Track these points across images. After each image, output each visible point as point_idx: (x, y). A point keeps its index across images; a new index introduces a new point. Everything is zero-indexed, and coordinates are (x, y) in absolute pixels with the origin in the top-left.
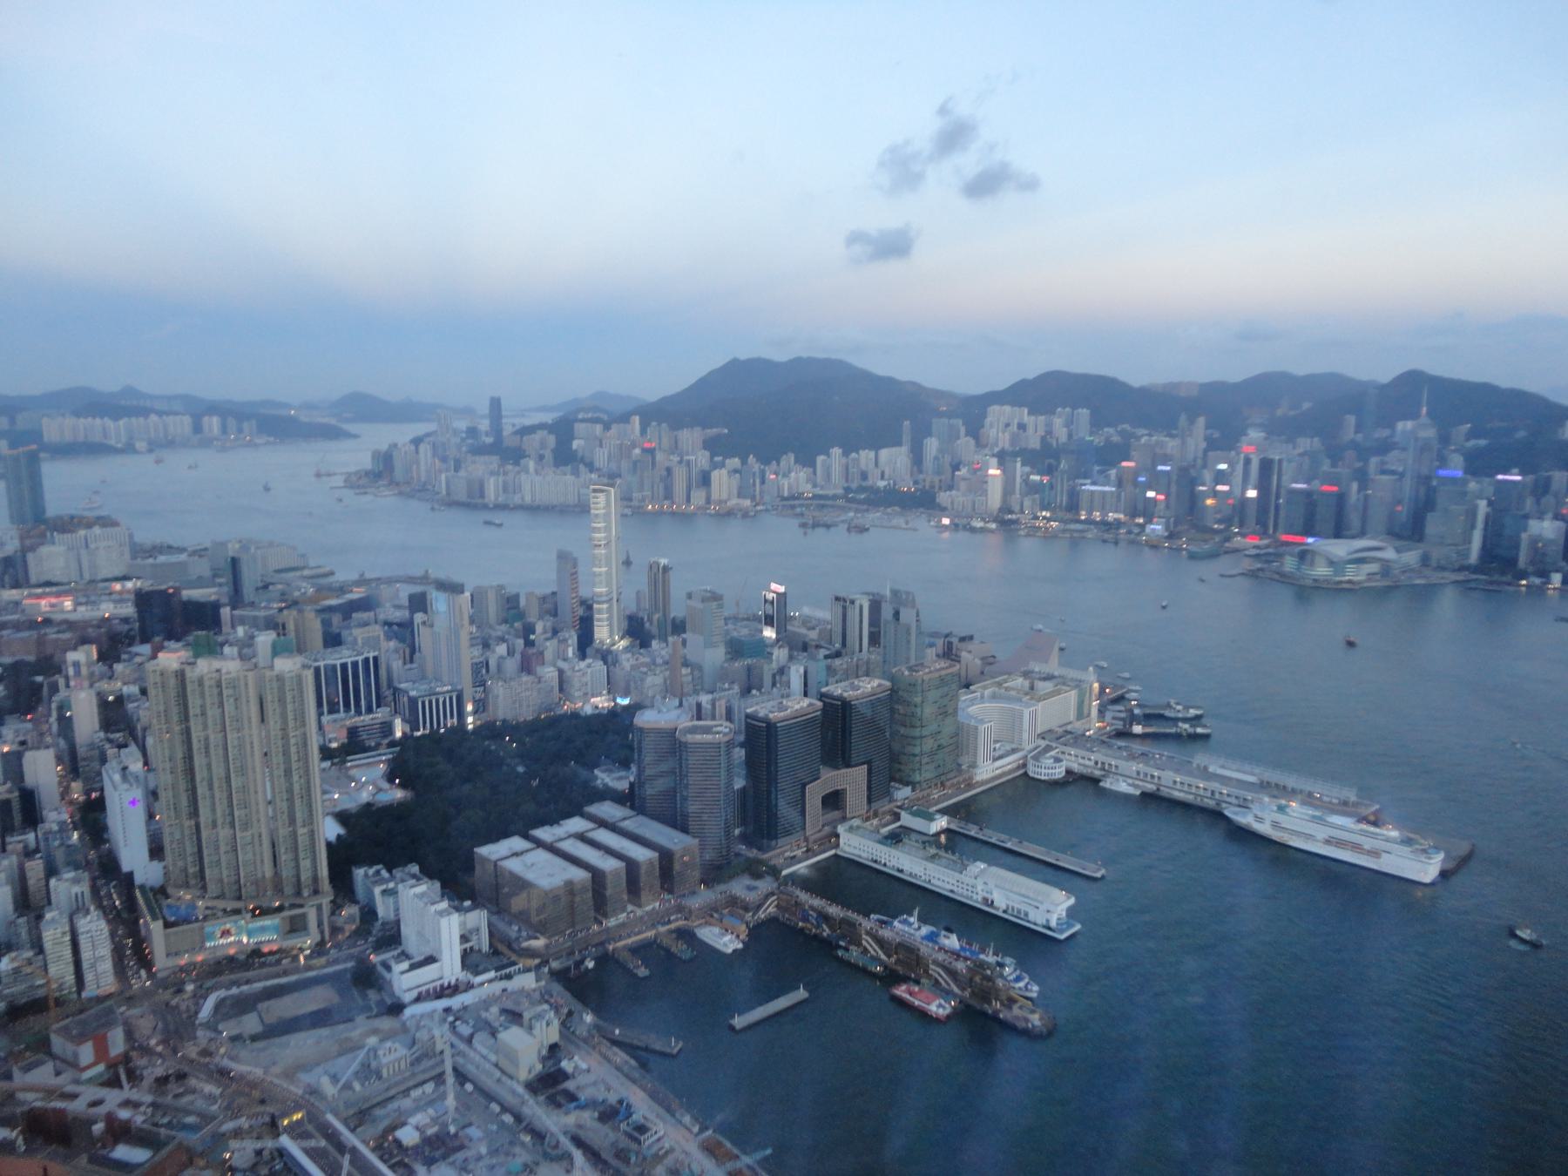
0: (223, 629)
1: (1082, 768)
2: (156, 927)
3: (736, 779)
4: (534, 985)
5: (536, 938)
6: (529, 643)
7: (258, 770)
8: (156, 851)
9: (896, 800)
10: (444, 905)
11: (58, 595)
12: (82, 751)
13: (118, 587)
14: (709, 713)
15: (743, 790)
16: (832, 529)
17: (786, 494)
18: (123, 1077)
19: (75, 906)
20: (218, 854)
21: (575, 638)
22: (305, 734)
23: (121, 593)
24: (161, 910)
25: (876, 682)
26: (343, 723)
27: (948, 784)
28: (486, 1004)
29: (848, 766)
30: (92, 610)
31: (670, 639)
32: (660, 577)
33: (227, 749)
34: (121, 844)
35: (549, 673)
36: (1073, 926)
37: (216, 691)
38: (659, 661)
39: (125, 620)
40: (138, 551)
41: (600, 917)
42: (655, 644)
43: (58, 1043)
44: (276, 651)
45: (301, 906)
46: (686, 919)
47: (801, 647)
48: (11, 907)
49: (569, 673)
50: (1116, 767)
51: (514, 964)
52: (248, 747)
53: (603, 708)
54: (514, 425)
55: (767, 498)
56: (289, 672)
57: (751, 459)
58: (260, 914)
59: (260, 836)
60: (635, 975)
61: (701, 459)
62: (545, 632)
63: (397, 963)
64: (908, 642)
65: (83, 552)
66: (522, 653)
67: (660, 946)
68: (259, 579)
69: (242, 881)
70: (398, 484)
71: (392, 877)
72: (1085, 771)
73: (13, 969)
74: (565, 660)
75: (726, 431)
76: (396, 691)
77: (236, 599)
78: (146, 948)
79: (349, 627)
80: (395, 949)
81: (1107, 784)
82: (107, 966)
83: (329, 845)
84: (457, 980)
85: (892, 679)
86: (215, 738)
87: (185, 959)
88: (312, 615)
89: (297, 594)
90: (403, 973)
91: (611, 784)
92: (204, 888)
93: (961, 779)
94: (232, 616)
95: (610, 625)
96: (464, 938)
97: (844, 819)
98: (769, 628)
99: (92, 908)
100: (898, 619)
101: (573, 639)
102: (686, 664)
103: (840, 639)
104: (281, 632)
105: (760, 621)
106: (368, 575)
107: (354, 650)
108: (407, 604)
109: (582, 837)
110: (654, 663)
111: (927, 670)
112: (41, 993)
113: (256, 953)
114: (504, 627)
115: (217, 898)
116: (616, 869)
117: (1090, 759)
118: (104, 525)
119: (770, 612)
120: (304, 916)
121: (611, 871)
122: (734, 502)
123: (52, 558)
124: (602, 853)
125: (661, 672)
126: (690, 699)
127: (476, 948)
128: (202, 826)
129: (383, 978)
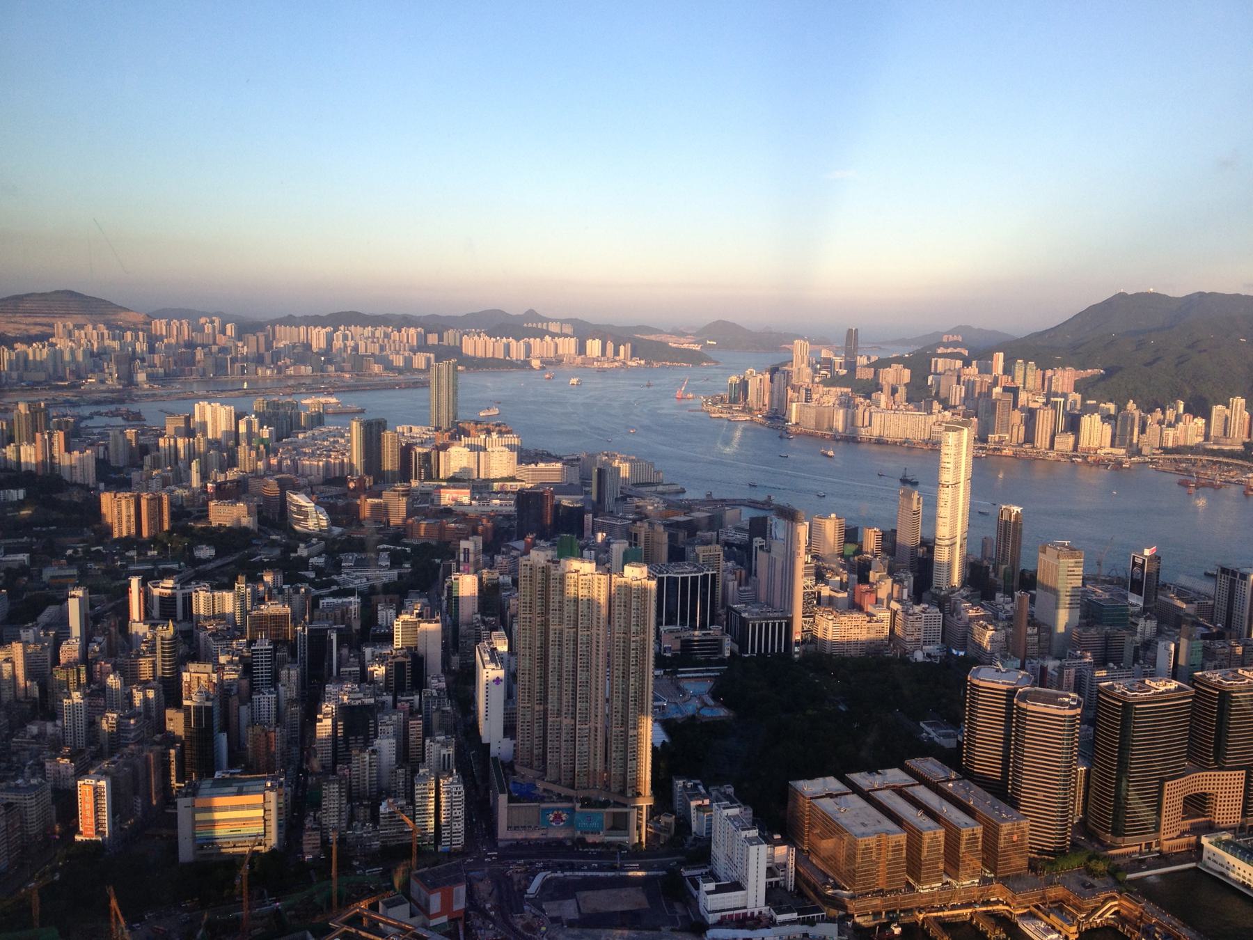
2: (503, 799)
7: (600, 668)
8: (510, 730)
10: (754, 833)
12: (462, 629)
14: (1055, 679)
17: (1170, 444)
18: (461, 933)
21: (912, 578)
22: (644, 640)
24: (508, 785)
31: (1017, 594)
39: (508, 517)
41: (911, 881)
42: (999, 597)
43: (415, 885)
44: (628, 559)
45: (625, 806)
46: (1007, 904)
51: (818, 910)
53: (935, 657)
55: (1146, 451)
57: (1131, 405)
58: (588, 806)
59: (596, 731)
67: (975, 928)
68: (619, 490)
69: (576, 770)
71: (708, 795)
73: (390, 813)
75: (1102, 371)
77: (598, 507)
79: (694, 545)
82: (460, 826)
84: (760, 913)
86: (568, 632)
87: (520, 835)
88: (662, 528)
90: (709, 893)
91: (936, 739)
92: (545, 771)
94: (593, 520)
96: (771, 871)
99: (454, 771)
101: (909, 581)
102: (1032, 622)
103: (1223, 617)
105: (1125, 587)
106: (715, 496)
107: (695, 566)
109: (900, 791)
110: (996, 618)
112: (407, 839)
113: (582, 841)
115: (554, 782)
119: (1139, 577)
120: (626, 815)
125: (1003, 628)
126: (1035, 662)
127: (782, 883)
128: (549, 712)
129: (693, 896)
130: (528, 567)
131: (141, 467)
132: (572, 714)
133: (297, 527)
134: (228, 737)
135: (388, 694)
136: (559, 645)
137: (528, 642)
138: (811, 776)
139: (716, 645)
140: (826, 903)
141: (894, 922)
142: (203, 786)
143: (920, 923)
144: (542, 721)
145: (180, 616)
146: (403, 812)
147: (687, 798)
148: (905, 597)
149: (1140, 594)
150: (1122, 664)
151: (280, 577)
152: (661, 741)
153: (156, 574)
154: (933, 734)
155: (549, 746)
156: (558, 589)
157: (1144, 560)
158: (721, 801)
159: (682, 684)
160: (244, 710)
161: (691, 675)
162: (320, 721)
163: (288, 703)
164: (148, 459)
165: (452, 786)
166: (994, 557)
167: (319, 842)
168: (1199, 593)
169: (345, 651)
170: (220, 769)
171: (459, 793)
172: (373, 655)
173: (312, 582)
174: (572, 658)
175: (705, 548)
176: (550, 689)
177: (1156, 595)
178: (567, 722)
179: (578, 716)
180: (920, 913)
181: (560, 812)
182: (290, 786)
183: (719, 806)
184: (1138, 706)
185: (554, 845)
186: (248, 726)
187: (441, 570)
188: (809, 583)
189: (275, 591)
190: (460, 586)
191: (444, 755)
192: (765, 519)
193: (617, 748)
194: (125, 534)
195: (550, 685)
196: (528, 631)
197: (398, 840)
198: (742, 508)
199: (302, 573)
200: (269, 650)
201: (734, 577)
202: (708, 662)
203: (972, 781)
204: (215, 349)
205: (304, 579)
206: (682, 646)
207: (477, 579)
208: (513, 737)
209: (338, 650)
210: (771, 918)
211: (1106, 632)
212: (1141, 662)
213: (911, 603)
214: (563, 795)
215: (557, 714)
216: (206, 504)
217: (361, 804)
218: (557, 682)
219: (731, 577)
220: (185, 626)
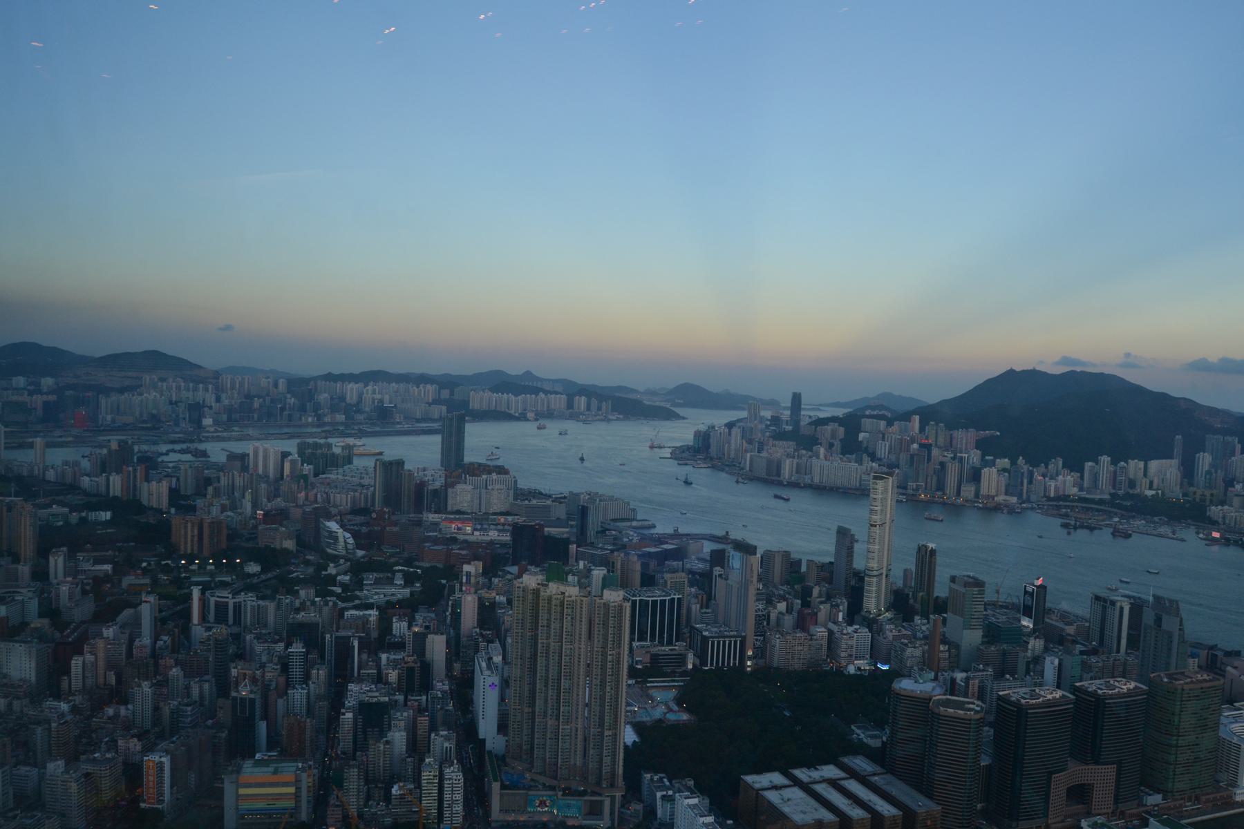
0: (570, 560)
2: (496, 786)
3: (983, 756)
6: (806, 604)
7: (581, 677)
8: (502, 728)
9: (1146, 805)
11: (464, 521)
12: (464, 639)
15: (989, 767)
16: (1096, 532)
17: (1052, 495)
19: (444, 759)
21: (846, 604)
22: (619, 654)
23: (504, 525)
25: (1132, 685)
26: (648, 649)
27: (1203, 798)
29: (1097, 763)
31: (931, 616)
32: (926, 558)
34: (481, 717)
35: (820, 632)
37: (559, 609)
38: (920, 635)
39: (503, 545)
42: (917, 620)
44: (606, 583)
45: (600, 795)
47: (1055, 639)
48: (405, 750)
52: (576, 659)
53: (865, 670)
54: (810, 417)
55: (1033, 498)
57: (1021, 460)
59: (577, 731)
61: (974, 457)
62: (820, 596)
64: (1170, 649)
66: (798, 613)
71: (671, 787)
73: (400, 794)
74: (835, 623)
75: (998, 433)
77: (581, 539)
82: (459, 808)
83: (626, 747)
85: (1149, 682)
87: (511, 817)
88: (636, 558)
89: (626, 540)
91: (865, 740)
92: (532, 763)
93: (1218, 795)
94: (577, 550)
95: (878, 598)
97: (1088, 814)
98: (1027, 619)
99: (455, 761)
100: (1160, 627)
101: (844, 605)
102: (944, 641)
105: (1019, 611)
107: (664, 591)
109: (834, 783)
110: (915, 637)
111: (1189, 680)
114: (784, 588)
115: (540, 774)
116: (863, 819)
118: (499, 473)
119: (1030, 604)
120: (602, 802)
121: (859, 820)
122: (1001, 498)
123: (463, 495)
124: (850, 802)
125: (921, 645)
126: (946, 674)
130: (521, 589)
131: (205, 496)
132: (556, 716)
133: (329, 551)
135: (399, 694)
136: (546, 657)
137: (519, 654)
138: (759, 771)
142: (245, 766)
144: (530, 721)
145: (231, 621)
146: (411, 794)
149: (1030, 617)
150: (1016, 676)
151: (312, 592)
152: (633, 740)
153: (213, 585)
154: (862, 736)
155: (536, 743)
157: (1033, 589)
159: (653, 692)
160: (280, 702)
162: (344, 714)
163: (317, 699)
164: (210, 489)
165: (453, 774)
166: (913, 584)
167: (341, 816)
168: (1077, 616)
169: (365, 656)
170: (258, 752)
171: (459, 780)
172: (388, 661)
173: (338, 596)
174: (557, 668)
175: (673, 575)
176: (537, 694)
177: (1043, 618)
181: (545, 798)
182: (317, 768)
183: (680, 796)
184: (1029, 711)
185: (539, 826)
186: (283, 717)
187: (446, 589)
188: (760, 606)
189: (308, 603)
190: (463, 604)
191: (447, 747)
192: (722, 552)
193: (594, 745)
194: (189, 551)
195: (538, 691)
196: (520, 644)
197: (407, 818)
198: (706, 543)
199: (332, 588)
200: (302, 652)
202: (673, 674)
203: (892, 774)
204: (268, 399)
205: (332, 594)
206: (651, 659)
207: (477, 598)
208: (505, 735)
209: (359, 655)
211: (1004, 649)
212: (1032, 674)
213: (845, 624)
215: (544, 716)
216: (255, 527)
217: (376, 787)
218: (544, 688)
219: (693, 600)
220: (235, 630)
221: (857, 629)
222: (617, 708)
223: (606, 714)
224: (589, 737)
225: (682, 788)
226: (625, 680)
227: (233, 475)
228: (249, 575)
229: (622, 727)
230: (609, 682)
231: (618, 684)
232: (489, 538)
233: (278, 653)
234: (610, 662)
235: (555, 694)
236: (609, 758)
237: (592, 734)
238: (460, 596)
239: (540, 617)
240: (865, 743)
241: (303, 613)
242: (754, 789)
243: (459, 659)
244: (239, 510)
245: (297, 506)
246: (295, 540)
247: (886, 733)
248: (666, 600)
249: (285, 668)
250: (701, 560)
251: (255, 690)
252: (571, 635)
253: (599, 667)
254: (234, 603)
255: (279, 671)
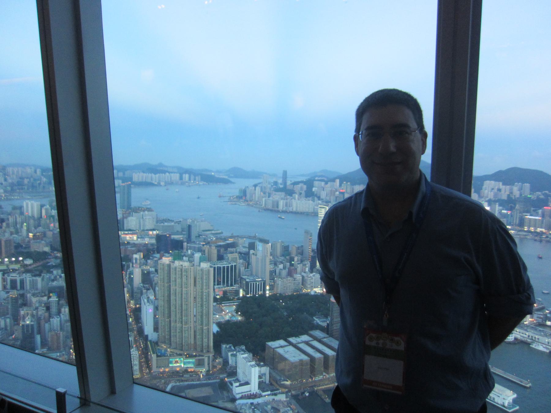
1: (522, 338)
2: (154, 356)
4: (285, 399)
5: (288, 381)
7: (192, 304)
8: (156, 329)
10: (253, 363)
11: (132, 234)
12: (135, 290)
13: (151, 233)
20: (176, 332)
21: (309, 264)
22: (209, 292)
26: (221, 289)
28: (266, 404)
30: (142, 240)
33: (182, 294)
35: (298, 277)
36: (516, 407)
39: (152, 245)
40: (158, 221)
41: (312, 376)
44: (201, 260)
45: (203, 356)
49: (306, 278)
50: (538, 339)
51: (278, 390)
52: (189, 295)
53: (318, 293)
56: (205, 268)
58: (188, 357)
59: (191, 328)
60: (325, 401)
62: (298, 261)
63: (235, 383)
65: (141, 220)
66: (289, 269)
70: (247, 201)
71: (235, 350)
72: (523, 339)
74: (305, 272)
76: (241, 278)
77: (189, 240)
78: (150, 363)
79: (226, 253)
80: (235, 377)
81: (533, 346)
83: (214, 334)
84: (256, 393)
86: (178, 290)
89: (209, 240)
90: (237, 387)
91: (320, 323)
92: (170, 344)
94: (187, 246)
96: (260, 377)
104: (203, 253)
106: (234, 235)
107: (228, 262)
108: (247, 245)
109: (307, 343)
113: (186, 371)
114: (282, 258)
115: (175, 349)
116: (320, 358)
117: (526, 334)
120: (203, 359)
121: (318, 358)
128: (172, 321)
129: (230, 388)
130: (162, 265)
134: (41, 336)
137: (162, 294)
139: (237, 292)
140: (281, 387)
141: (305, 392)
143: (315, 391)
144: (169, 325)
145: (19, 287)
147: (227, 352)
148: (307, 271)
152: (216, 330)
154: (318, 321)
156: (174, 273)
158: (240, 352)
160: (47, 325)
161: (228, 304)
164: (4, 224)
165: (133, 352)
170: (38, 349)
171: (136, 355)
178: (179, 325)
179: (183, 322)
180: (315, 387)
182: (67, 355)
183: (240, 354)
186: (49, 332)
187: (126, 266)
188: (271, 267)
189: (58, 277)
193: (199, 334)
201: (242, 266)
203: (333, 337)
204: (32, 179)
207: (141, 270)
208: (157, 332)
210: (260, 394)
214: (178, 353)
216: (29, 242)
220: (21, 292)
221: (314, 275)
222: (209, 316)
223: (204, 319)
224: (197, 330)
225: (240, 350)
226: (212, 303)
227: (16, 217)
228: (27, 265)
229: (212, 325)
230: (205, 305)
231: (209, 305)
232: (144, 242)
233: (44, 302)
234: (205, 295)
235: (180, 311)
236: (206, 339)
237: (198, 329)
238: (132, 269)
239: (172, 277)
240: (320, 324)
241: (55, 282)
242: (272, 348)
243: (133, 299)
244: (20, 234)
245: (50, 231)
246: (50, 246)
247: (329, 320)
248: (229, 266)
249: (48, 308)
250: (244, 247)
251: (33, 320)
252: (186, 284)
253: (200, 298)
254: (20, 279)
255: (45, 310)
